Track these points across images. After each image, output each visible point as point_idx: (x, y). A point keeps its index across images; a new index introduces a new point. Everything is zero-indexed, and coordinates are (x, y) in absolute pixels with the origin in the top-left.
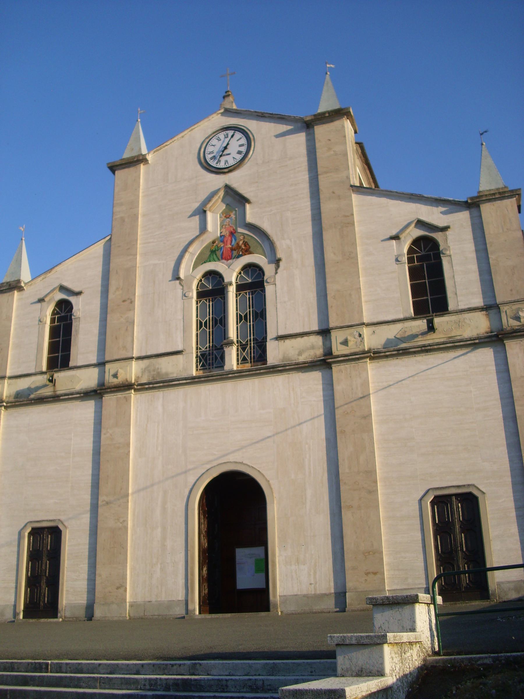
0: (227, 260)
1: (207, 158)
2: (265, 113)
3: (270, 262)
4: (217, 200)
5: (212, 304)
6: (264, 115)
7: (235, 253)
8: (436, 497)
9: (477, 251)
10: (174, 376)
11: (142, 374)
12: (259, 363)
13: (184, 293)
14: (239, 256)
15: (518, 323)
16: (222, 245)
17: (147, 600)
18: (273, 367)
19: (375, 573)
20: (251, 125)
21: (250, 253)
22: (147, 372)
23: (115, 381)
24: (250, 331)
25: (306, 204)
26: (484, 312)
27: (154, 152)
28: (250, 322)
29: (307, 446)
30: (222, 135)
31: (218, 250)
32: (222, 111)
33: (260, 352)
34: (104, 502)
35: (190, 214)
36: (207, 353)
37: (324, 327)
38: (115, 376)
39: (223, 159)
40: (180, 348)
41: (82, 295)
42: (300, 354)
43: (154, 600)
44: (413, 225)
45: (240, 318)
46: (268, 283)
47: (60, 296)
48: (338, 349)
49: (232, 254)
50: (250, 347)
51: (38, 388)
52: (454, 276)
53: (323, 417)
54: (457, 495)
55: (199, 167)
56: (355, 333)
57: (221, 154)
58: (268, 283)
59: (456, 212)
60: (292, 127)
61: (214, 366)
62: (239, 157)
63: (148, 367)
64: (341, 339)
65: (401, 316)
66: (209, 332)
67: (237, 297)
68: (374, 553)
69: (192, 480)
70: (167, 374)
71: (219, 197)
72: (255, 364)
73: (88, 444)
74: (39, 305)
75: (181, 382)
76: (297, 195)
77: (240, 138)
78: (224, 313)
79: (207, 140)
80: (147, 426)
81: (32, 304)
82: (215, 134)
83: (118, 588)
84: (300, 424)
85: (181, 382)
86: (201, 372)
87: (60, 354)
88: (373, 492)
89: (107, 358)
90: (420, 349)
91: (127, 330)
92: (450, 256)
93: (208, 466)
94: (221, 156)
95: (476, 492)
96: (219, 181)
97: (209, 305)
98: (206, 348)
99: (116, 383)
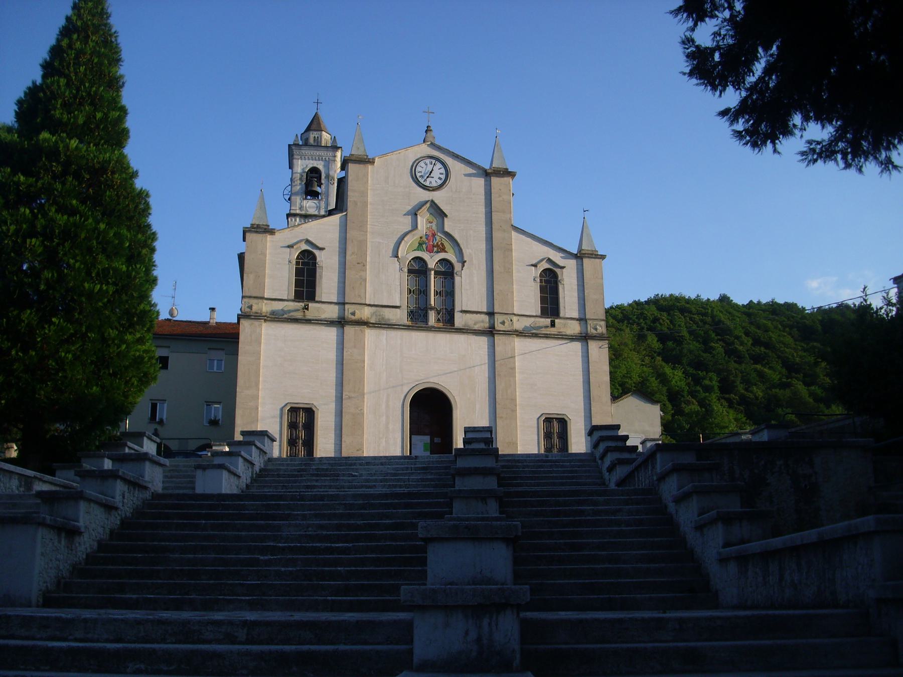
3: (458, 262)
4: (425, 209)
7: (435, 249)
8: (546, 418)
9: (578, 285)
10: (394, 322)
11: (371, 317)
12: (448, 325)
14: (438, 252)
15: (595, 332)
18: (456, 329)
20: (449, 161)
21: (446, 252)
22: (374, 315)
23: (353, 318)
25: (482, 229)
26: (578, 322)
30: (428, 161)
34: (347, 396)
35: (404, 213)
36: (415, 311)
37: (490, 311)
38: (353, 314)
39: (429, 179)
40: (398, 305)
41: (324, 250)
42: (475, 324)
44: (545, 260)
45: (436, 293)
47: (305, 247)
48: (499, 326)
49: (433, 250)
50: (443, 313)
51: (290, 311)
54: (556, 419)
57: (427, 175)
60: (475, 172)
62: (440, 182)
65: (534, 314)
68: (513, 444)
69: (406, 390)
70: (389, 320)
72: (446, 324)
73: (332, 355)
74: (288, 250)
76: (478, 221)
77: (441, 168)
78: (426, 287)
79: (417, 162)
81: (281, 247)
82: (422, 159)
83: (358, 450)
84: (473, 367)
86: (410, 322)
88: (514, 411)
89: (346, 301)
92: (564, 285)
94: (428, 177)
95: (566, 419)
96: (426, 196)
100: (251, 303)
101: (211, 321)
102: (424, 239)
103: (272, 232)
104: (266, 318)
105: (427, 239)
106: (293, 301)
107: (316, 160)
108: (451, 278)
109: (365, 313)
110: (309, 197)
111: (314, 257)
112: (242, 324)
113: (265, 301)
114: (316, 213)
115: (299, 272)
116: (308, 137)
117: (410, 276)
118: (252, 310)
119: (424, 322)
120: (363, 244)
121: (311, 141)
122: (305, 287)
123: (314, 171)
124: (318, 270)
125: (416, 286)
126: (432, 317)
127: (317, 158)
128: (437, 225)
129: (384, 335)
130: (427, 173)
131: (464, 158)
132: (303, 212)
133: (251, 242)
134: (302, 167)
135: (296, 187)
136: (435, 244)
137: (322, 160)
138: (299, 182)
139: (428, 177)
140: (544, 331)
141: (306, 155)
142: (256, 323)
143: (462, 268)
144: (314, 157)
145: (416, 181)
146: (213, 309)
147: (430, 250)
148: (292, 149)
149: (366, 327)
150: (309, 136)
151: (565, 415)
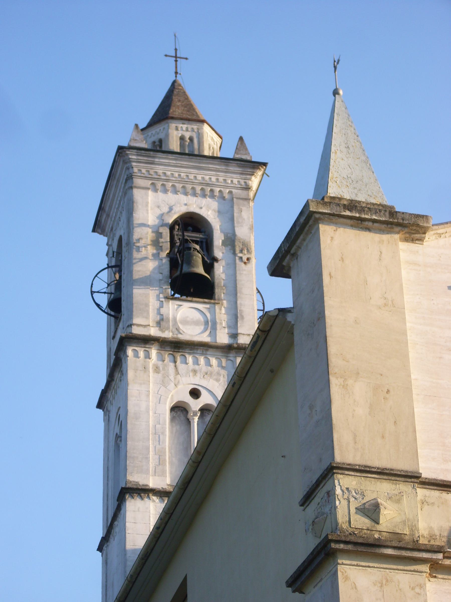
100: (369, 497)
104: (440, 556)
107: (195, 194)
110: (177, 295)
112: (347, 578)
113: (422, 492)
114: (205, 338)
116: (162, 136)
118: (377, 522)
121: (175, 146)
127: (198, 188)
132: (168, 335)
133: (342, 259)
134: (158, 212)
135: (143, 262)
137: (212, 196)
138: (151, 250)
141: (168, 180)
144: (189, 187)
148: (130, 161)
150: (167, 135)
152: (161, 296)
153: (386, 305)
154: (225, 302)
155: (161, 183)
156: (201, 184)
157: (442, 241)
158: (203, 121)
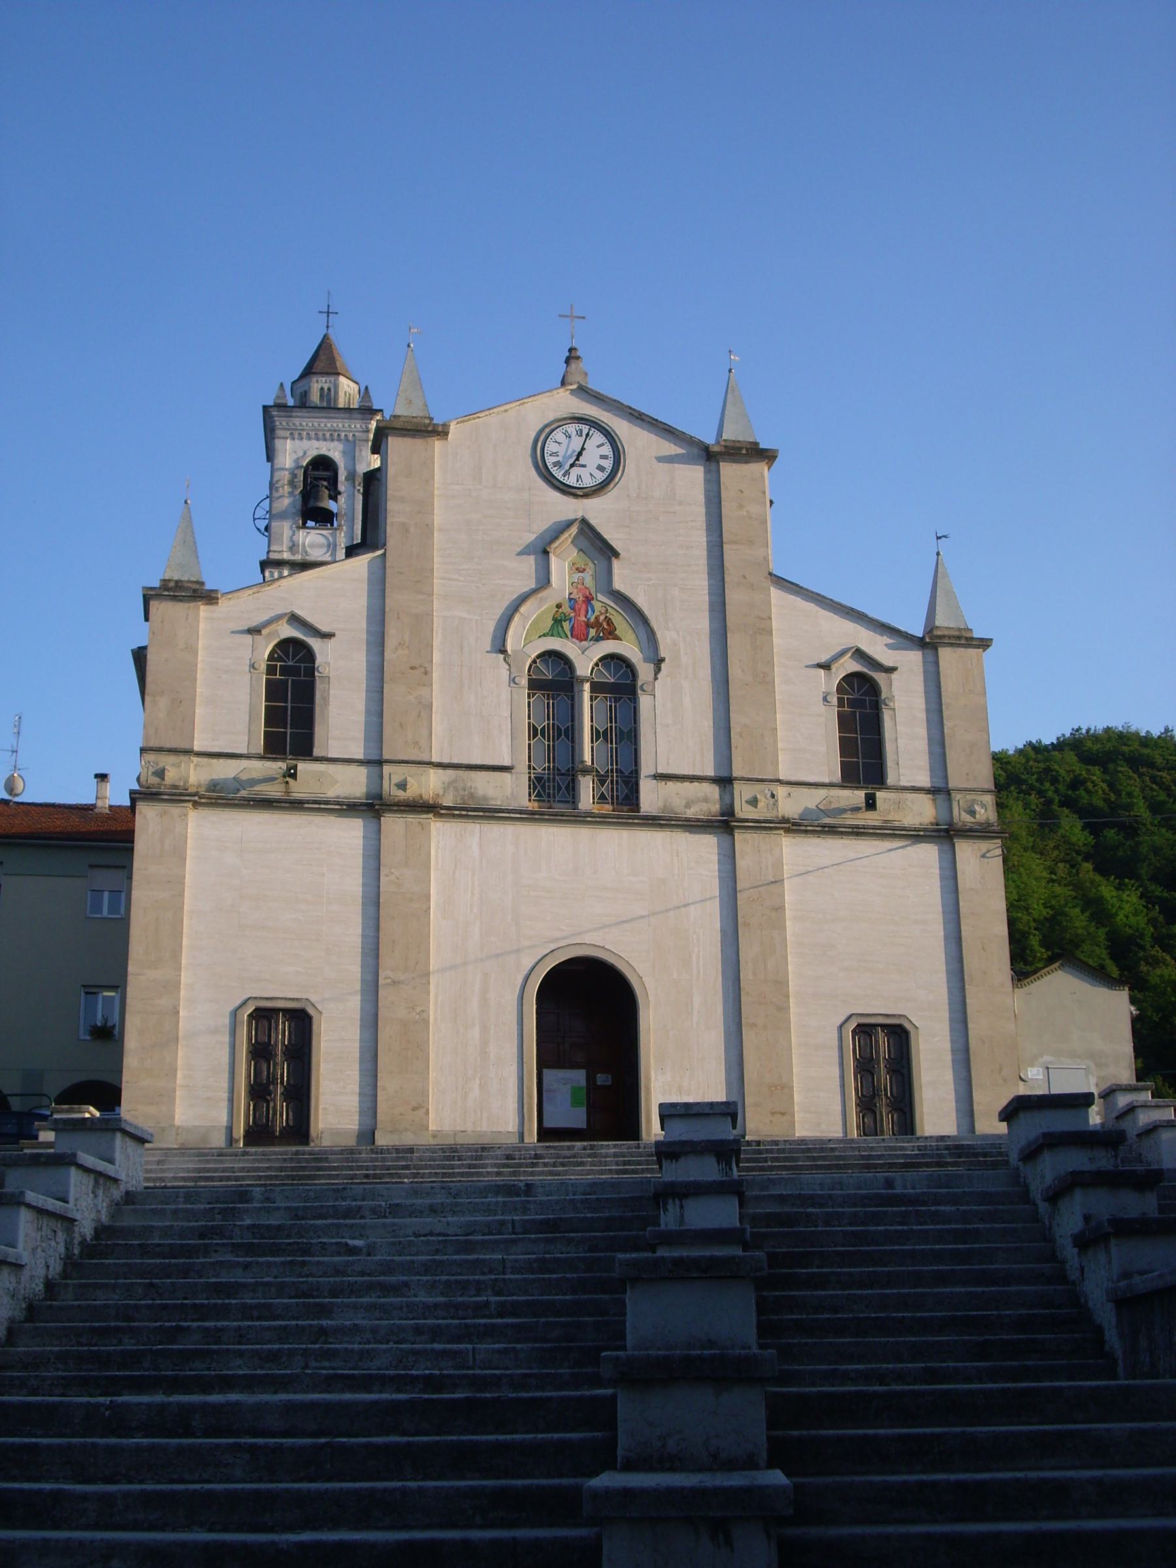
0: (581, 640)
1: (547, 461)
2: (644, 414)
3: (646, 660)
4: (567, 538)
5: (553, 703)
6: (643, 417)
7: (592, 632)
9: (928, 711)
10: (497, 803)
11: (444, 792)
12: (625, 808)
13: (512, 677)
14: (597, 639)
15: (972, 820)
16: (572, 615)
17: (459, 1128)
18: (646, 818)
19: (783, 1114)
20: (621, 427)
21: (617, 638)
22: (452, 789)
23: (401, 795)
24: (612, 756)
25: (701, 582)
26: (929, 796)
27: (458, 423)
28: (612, 743)
29: (695, 936)
30: (572, 428)
31: (565, 621)
32: (574, 387)
33: (626, 791)
34: (389, 980)
36: (546, 776)
37: (725, 774)
38: (402, 786)
39: (575, 471)
40: (506, 762)
41: (333, 639)
42: (688, 806)
43: (469, 1127)
44: (850, 655)
45: (596, 735)
46: (644, 691)
47: (287, 631)
48: (743, 810)
49: (588, 633)
50: (612, 781)
51: (253, 782)
52: (896, 739)
53: (717, 901)
54: (883, 1026)
55: (534, 472)
56: (766, 791)
57: (571, 461)
58: (644, 691)
59: (906, 649)
60: (684, 452)
61: (557, 799)
62: (601, 477)
63: (455, 781)
64: (747, 796)
65: (827, 780)
66: (549, 745)
67: (591, 700)
68: (783, 1088)
69: (528, 963)
70: (485, 798)
71: (570, 535)
72: (620, 807)
73: (354, 884)
74: (248, 638)
75: (512, 815)
77: (602, 445)
78: (573, 720)
79: (547, 430)
80: (454, 872)
81: (232, 632)
82: (561, 423)
83: (414, 1109)
84: (685, 906)
85: (512, 815)
86: (536, 804)
87: (289, 731)
88: (784, 1009)
89: (386, 756)
90: (850, 830)
91: (419, 716)
92: (894, 709)
93: (553, 947)
94: (572, 466)
95: (907, 1026)
96: (571, 508)
97: (548, 704)
98: (544, 769)
99: (402, 798)
100: (161, 765)
101: (100, 803)
102: (566, 609)
103: (210, 598)
104: (196, 798)
105: (573, 608)
106: (261, 758)
107: (325, 440)
108: (629, 699)
109: (431, 784)
110: (310, 523)
111: (310, 656)
112: (141, 813)
113: (195, 759)
115: (274, 691)
116: (306, 388)
117: (534, 694)
118: (164, 780)
119: (569, 802)
120: (422, 623)
121: (315, 398)
122: (289, 726)
123: (322, 466)
124: (319, 687)
125: (549, 719)
126: (587, 788)
127: (328, 435)
128: (595, 577)
129: (475, 833)
130: (571, 457)
131: (657, 420)
132: (298, 558)
133: (162, 622)
134: (295, 457)
135: (280, 500)
136: (592, 619)
137: (339, 440)
138: (287, 489)
139: (572, 466)
140: (851, 820)
141: (303, 430)
142: (175, 810)
143: (656, 674)
144: (320, 434)
145: (546, 474)
146: (102, 777)
147: (579, 635)
148: (273, 417)
149: (431, 815)
151: (905, 1016)
152: (294, 526)
153: (186, 648)
154: (344, 527)
155: (298, 432)
156: (329, 430)
157: (231, 602)
158: (339, 374)
